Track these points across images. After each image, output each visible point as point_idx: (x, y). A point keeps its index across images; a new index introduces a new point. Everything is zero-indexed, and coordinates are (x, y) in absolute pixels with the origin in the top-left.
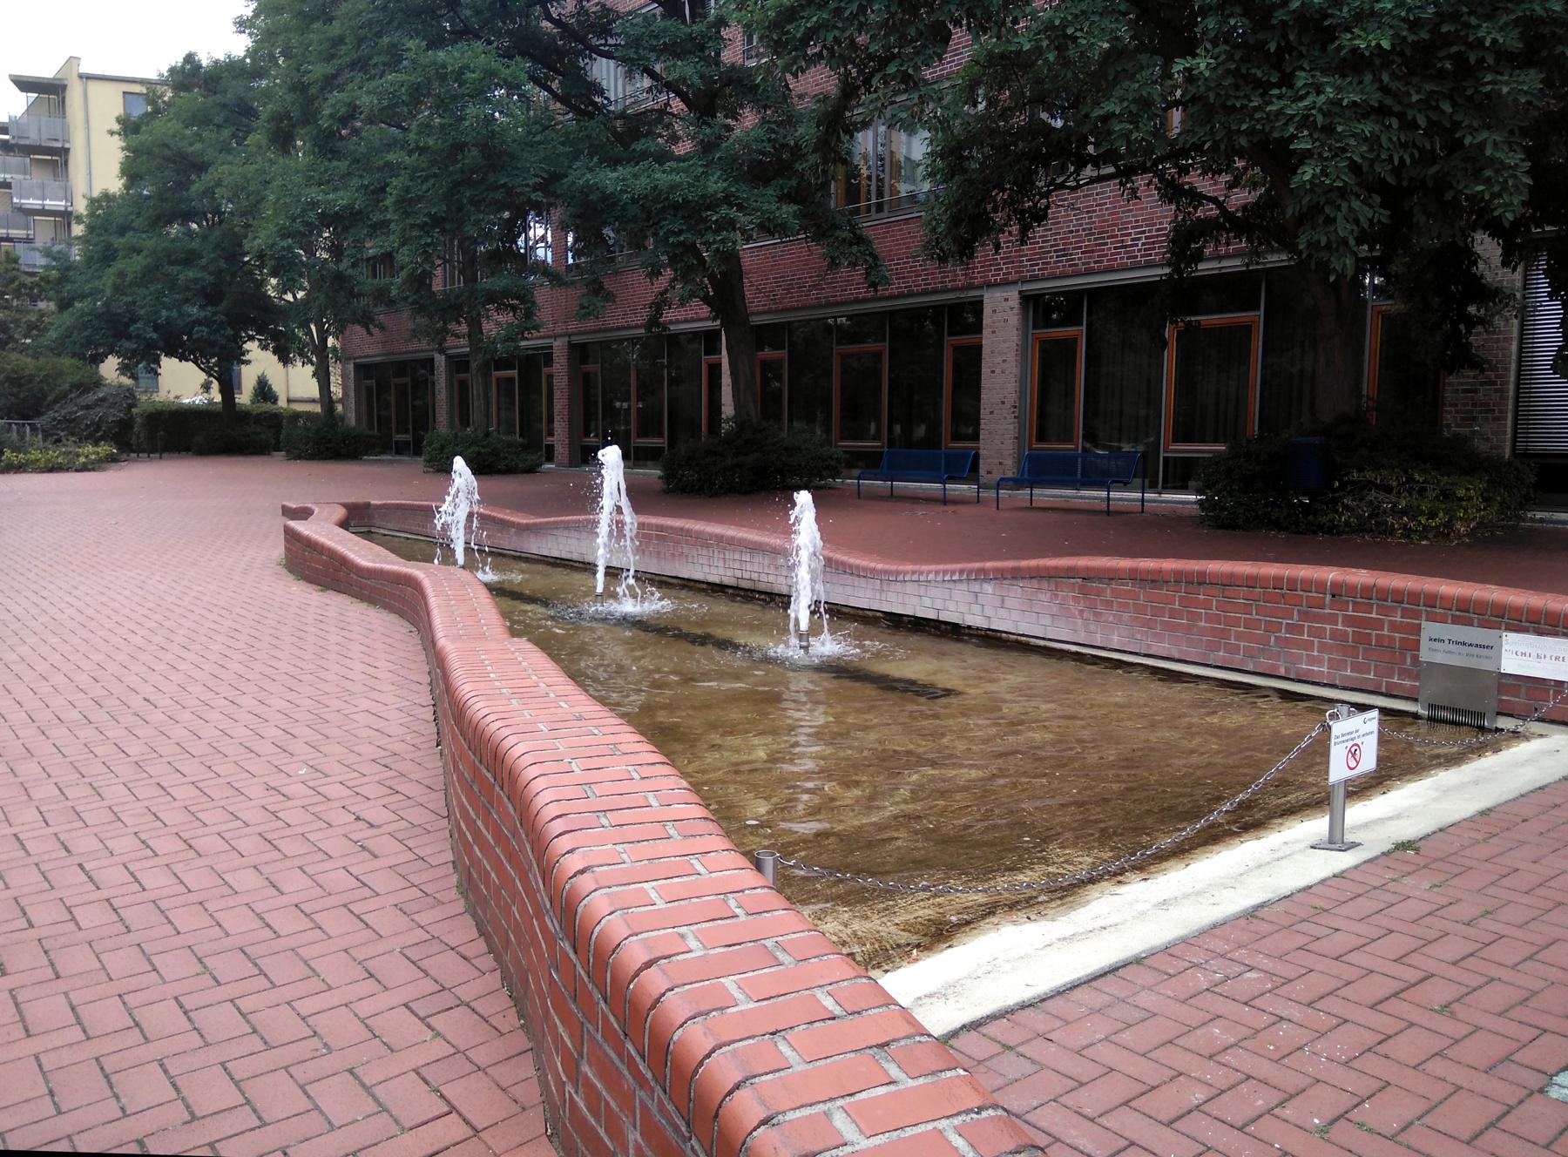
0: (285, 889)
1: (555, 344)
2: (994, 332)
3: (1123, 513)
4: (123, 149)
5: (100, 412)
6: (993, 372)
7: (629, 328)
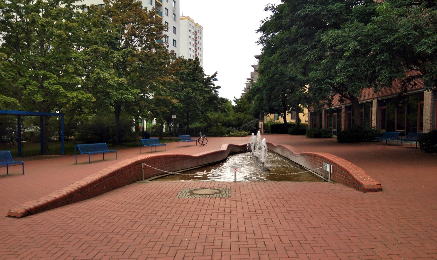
0: (295, 224)
1: (343, 106)
2: (426, 100)
3: (145, 153)
4: (218, 94)
5: (251, 125)
6: (426, 111)
7: (365, 100)
